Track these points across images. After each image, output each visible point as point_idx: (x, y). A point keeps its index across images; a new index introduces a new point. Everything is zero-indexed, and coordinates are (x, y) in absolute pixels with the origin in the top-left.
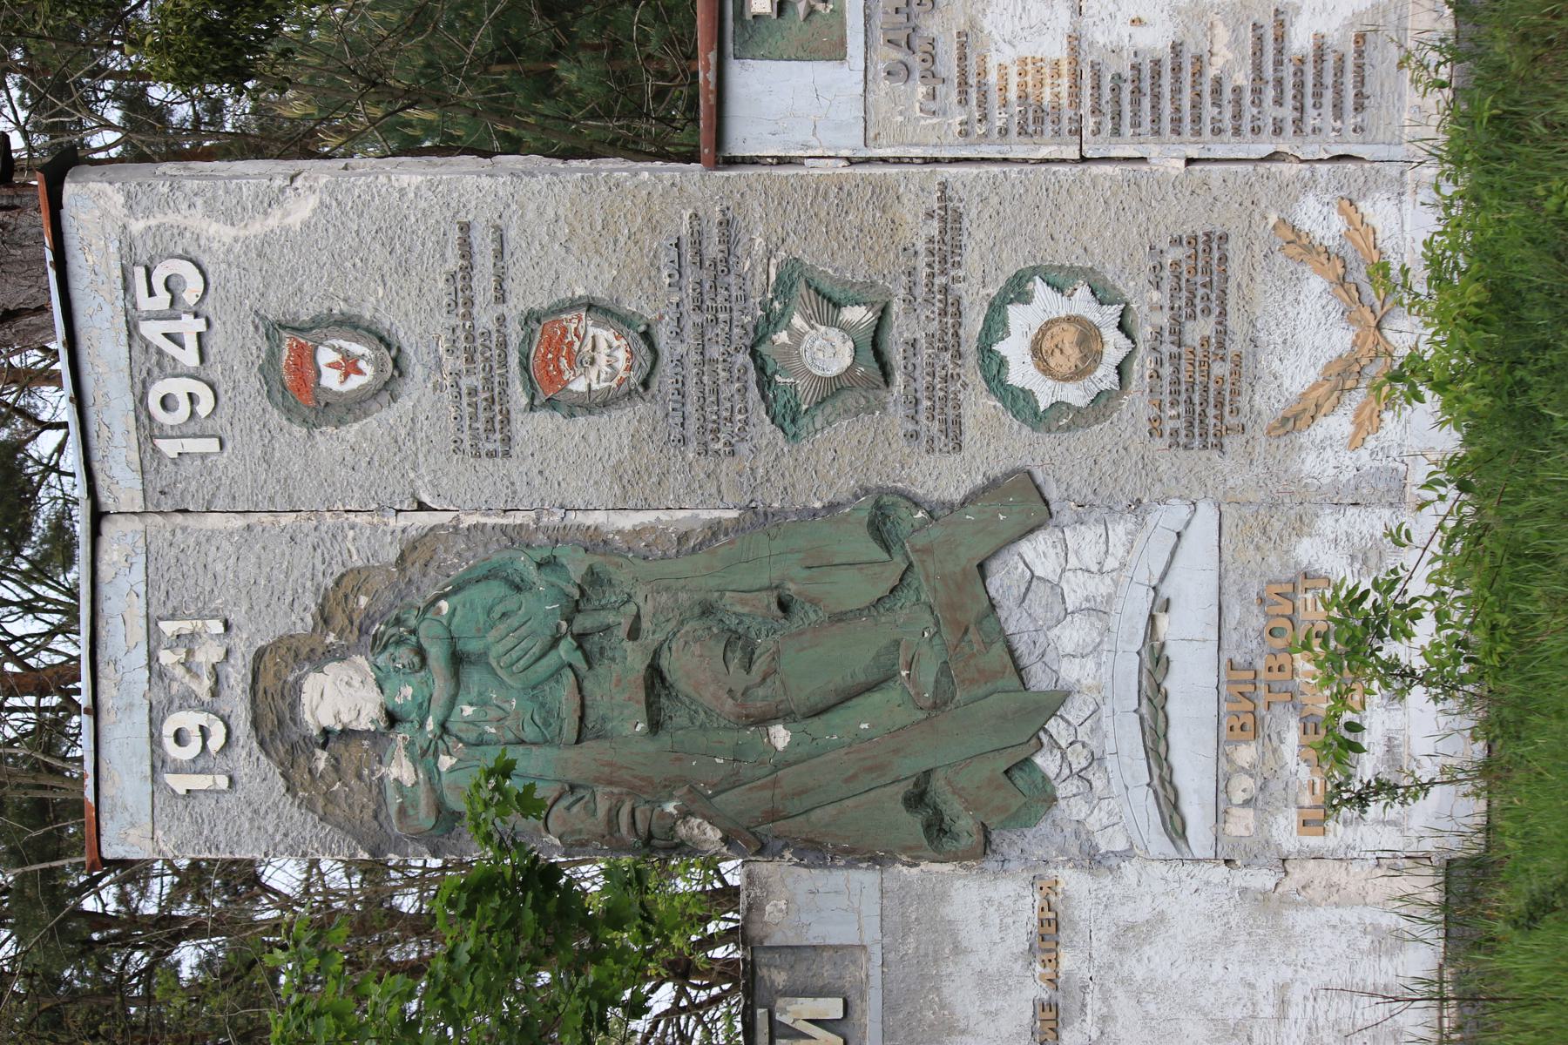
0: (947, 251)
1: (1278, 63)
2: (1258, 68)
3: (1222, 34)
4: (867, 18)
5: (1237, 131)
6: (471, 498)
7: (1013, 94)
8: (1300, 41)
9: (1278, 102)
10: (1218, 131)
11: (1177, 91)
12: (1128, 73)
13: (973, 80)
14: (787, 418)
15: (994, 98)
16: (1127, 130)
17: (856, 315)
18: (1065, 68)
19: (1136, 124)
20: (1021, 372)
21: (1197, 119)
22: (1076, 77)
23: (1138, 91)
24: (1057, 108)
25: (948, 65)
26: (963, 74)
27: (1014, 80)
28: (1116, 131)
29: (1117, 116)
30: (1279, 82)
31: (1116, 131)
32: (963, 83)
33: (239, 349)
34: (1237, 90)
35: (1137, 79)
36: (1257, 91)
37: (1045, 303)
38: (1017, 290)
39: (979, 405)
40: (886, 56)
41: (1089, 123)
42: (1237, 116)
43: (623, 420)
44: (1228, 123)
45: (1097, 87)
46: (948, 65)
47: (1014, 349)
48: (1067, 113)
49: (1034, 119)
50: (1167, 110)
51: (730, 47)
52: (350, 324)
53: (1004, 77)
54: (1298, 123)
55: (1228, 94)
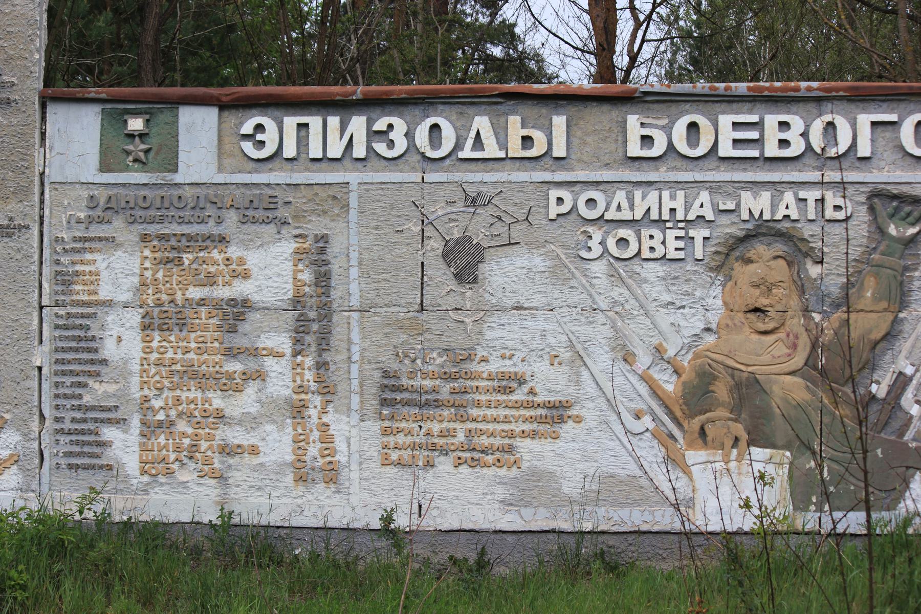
1: (95, 420)
2: (93, 408)
3: (112, 388)
4: (124, 185)
5: (57, 396)
7: (79, 268)
8: (109, 433)
9: (73, 420)
10: (57, 385)
11: (79, 362)
12: (90, 334)
13: (87, 245)
15: (77, 257)
16: (57, 333)
18: (94, 298)
19: (61, 338)
21: (64, 373)
22: (88, 304)
23: (80, 339)
24: (71, 293)
25: (96, 231)
26: (91, 239)
27: (87, 268)
28: (57, 327)
29: (66, 328)
30: (85, 421)
31: (57, 327)
32: (86, 239)
34: (80, 397)
35: (87, 339)
36: (79, 408)
40: (102, 195)
41: (62, 312)
42: (66, 396)
44: (62, 391)
45: (83, 316)
46: (96, 231)
48: (68, 299)
49: (65, 280)
50: (69, 356)
51: (109, 106)
53: (89, 263)
54: (60, 431)
55: (78, 391)
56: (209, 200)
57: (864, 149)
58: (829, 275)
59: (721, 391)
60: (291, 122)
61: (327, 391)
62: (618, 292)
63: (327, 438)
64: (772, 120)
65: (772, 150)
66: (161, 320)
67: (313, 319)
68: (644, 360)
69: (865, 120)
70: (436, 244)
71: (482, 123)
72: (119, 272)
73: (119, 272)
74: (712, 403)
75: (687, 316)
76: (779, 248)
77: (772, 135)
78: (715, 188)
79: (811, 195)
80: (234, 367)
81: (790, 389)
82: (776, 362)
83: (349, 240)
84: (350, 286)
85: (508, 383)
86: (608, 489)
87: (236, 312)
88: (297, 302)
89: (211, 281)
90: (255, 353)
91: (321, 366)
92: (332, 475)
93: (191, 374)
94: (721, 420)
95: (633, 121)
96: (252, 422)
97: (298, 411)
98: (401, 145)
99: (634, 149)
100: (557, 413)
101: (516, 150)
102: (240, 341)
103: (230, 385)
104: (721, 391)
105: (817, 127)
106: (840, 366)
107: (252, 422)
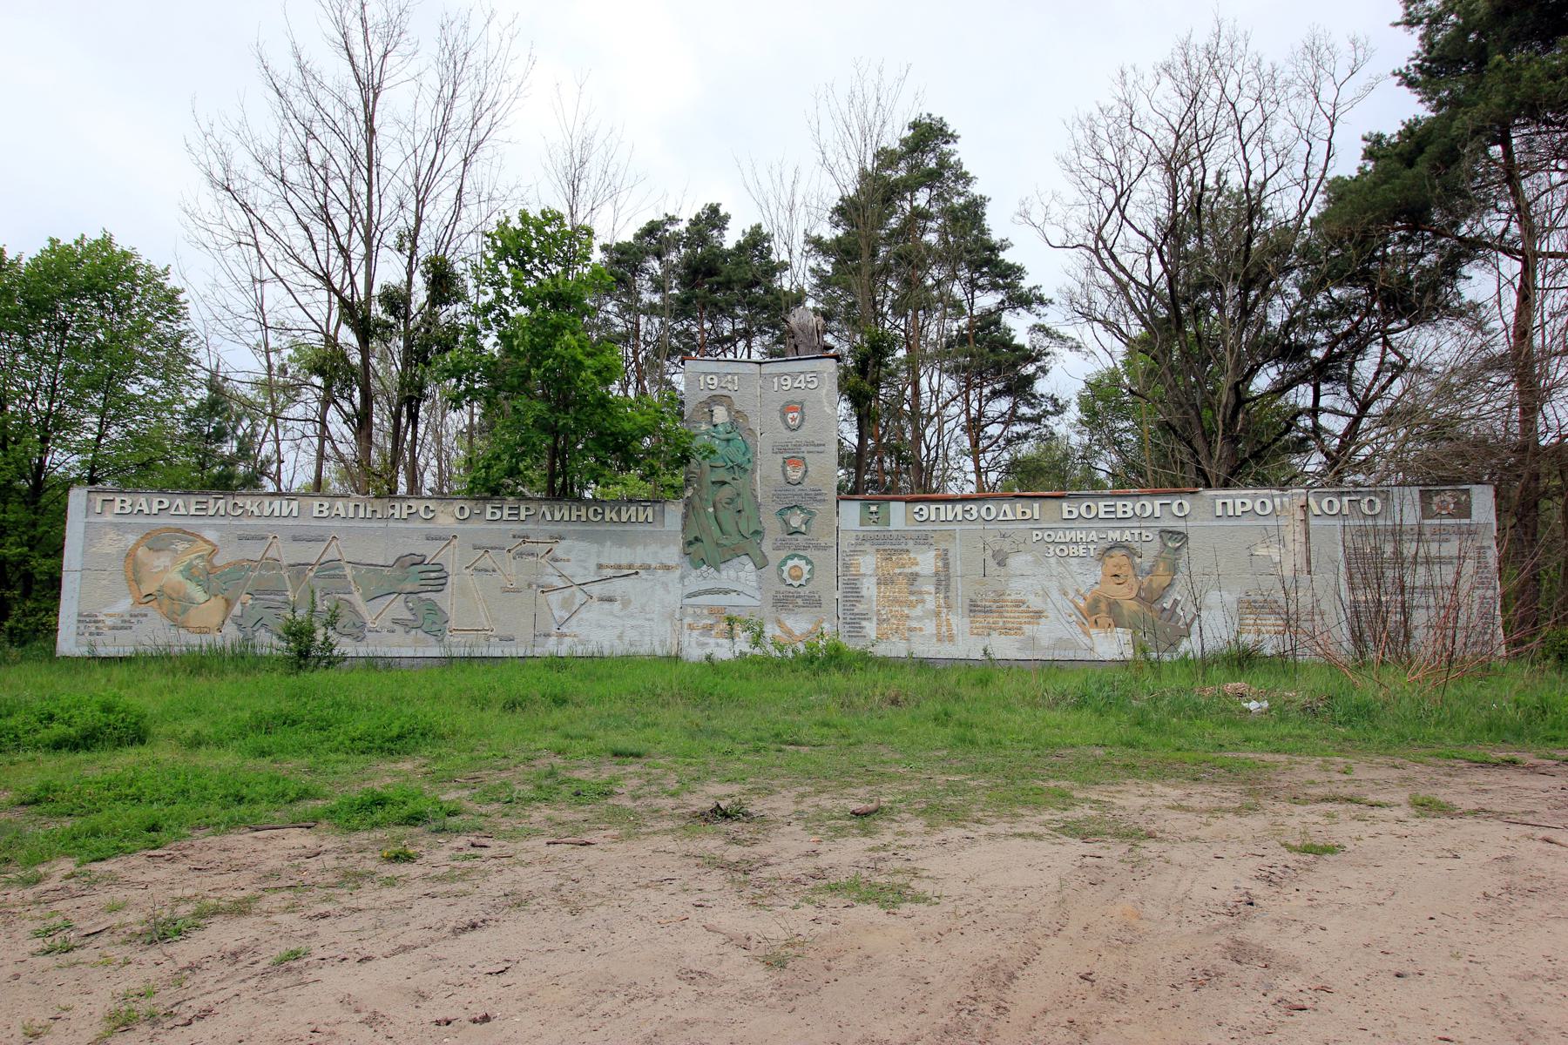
0: (817, 547)
6: (763, 445)
8: (864, 623)
14: (781, 513)
17: (803, 529)
20: (790, 563)
33: (797, 396)
37: (807, 568)
38: (809, 562)
39: (783, 554)
43: (781, 478)
47: (796, 561)
52: (803, 420)
56: (903, 536)
57: (1157, 514)
58: (1145, 562)
59: (1103, 606)
60: (933, 507)
61: (949, 607)
62: (1061, 569)
63: (949, 625)
64: (1120, 504)
65: (1120, 515)
66: (884, 581)
67: (943, 580)
68: (1071, 595)
69: (1157, 503)
70: (989, 552)
71: (1006, 507)
72: (868, 563)
73: (868, 563)
74: (1100, 611)
75: (1089, 578)
76: (1124, 552)
77: (1120, 510)
78: (1098, 530)
79: (1137, 532)
80: (913, 598)
81: (1130, 606)
82: (1124, 594)
83: (956, 551)
84: (957, 567)
85: (1019, 603)
86: (1060, 643)
87: (914, 577)
88: (937, 574)
89: (903, 566)
90: (921, 593)
91: (946, 597)
92: (951, 638)
93: (896, 601)
94: (1104, 618)
95: (1065, 505)
96: (920, 619)
97: (938, 614)
98: (975, 515)
99: (1066, 516)
100: (1038, 614)
101: (1020, 516)
102: (914, 589)
103: (911, 605)
104: (1103, 606)
105: (1138, 506)
106: (1149, 598)
107: (920, 619)
